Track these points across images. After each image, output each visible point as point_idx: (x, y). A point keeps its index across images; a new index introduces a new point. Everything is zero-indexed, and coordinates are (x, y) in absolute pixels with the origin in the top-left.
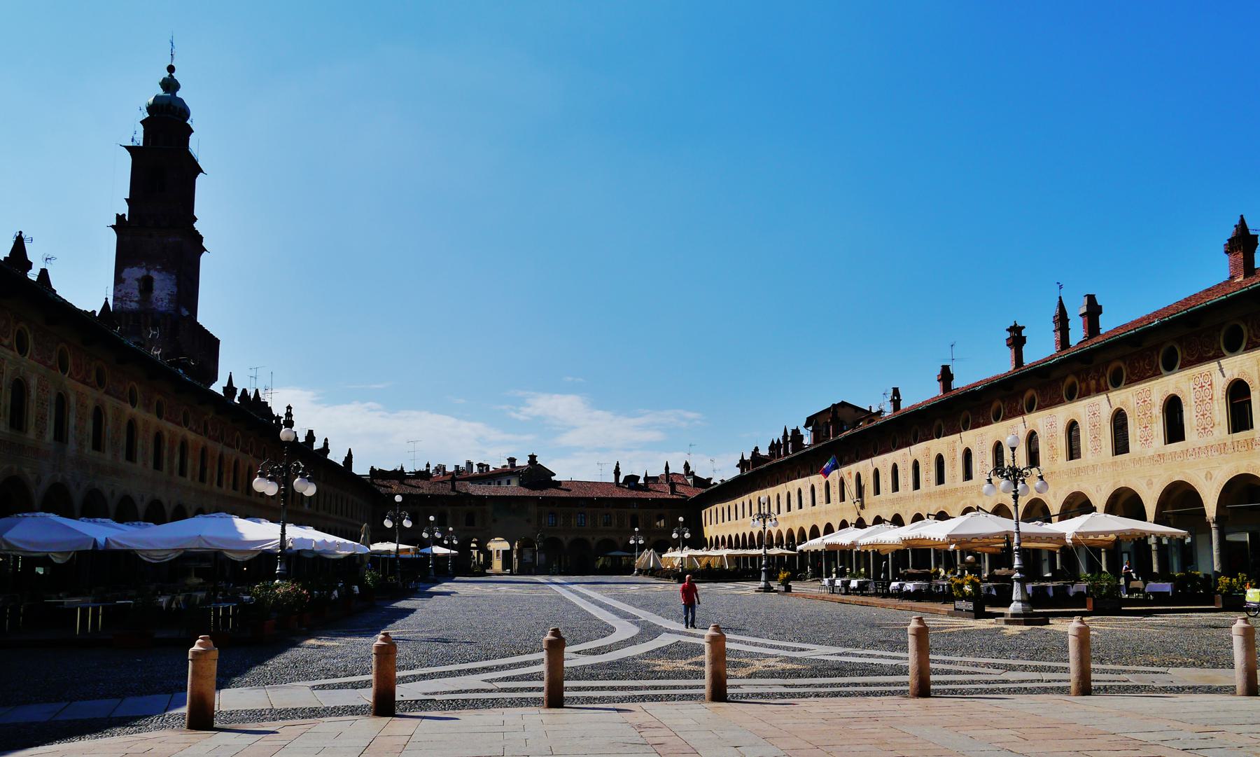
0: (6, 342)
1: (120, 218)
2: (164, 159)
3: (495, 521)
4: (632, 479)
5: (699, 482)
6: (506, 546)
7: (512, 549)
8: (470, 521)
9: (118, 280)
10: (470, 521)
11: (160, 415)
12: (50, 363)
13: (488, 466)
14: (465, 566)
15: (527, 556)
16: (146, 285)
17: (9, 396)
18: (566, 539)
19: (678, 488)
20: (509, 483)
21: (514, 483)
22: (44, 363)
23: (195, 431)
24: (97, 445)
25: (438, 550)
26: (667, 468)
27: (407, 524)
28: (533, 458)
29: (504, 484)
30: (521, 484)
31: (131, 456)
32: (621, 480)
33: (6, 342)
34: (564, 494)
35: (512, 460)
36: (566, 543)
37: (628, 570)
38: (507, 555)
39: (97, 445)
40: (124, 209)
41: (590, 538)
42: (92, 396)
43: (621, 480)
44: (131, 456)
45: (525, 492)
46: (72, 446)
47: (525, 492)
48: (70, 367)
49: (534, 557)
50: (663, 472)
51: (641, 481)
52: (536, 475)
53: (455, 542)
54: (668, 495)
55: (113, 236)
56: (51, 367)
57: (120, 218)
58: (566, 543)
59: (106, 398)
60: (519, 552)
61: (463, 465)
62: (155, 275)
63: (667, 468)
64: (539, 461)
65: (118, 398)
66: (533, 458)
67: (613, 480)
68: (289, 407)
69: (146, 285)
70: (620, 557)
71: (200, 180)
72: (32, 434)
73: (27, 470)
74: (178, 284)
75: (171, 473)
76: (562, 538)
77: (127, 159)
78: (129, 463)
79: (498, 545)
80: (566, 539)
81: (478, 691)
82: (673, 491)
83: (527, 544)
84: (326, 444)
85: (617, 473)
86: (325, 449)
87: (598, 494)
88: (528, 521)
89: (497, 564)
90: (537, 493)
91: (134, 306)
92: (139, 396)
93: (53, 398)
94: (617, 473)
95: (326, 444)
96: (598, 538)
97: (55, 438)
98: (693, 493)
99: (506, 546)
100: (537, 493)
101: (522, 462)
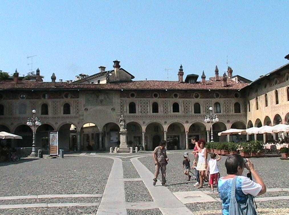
3: (86, 109)
4: (192, 78)
5: (240, 79)
8: (67, 109)
10: (67, 109)
21: (104, 82)
26: (217, 72)
28: (117, 64)
32: (184, 81)
50: (214, 75)
51: (199, 79)
63: (217, 72)
66: (117, 64)
76: (140, 122)
85: (181, 73)
87: (166, 88)
88: (113, 109)
94: (181, 73)
98: (241, 86)
101: (110, 67)
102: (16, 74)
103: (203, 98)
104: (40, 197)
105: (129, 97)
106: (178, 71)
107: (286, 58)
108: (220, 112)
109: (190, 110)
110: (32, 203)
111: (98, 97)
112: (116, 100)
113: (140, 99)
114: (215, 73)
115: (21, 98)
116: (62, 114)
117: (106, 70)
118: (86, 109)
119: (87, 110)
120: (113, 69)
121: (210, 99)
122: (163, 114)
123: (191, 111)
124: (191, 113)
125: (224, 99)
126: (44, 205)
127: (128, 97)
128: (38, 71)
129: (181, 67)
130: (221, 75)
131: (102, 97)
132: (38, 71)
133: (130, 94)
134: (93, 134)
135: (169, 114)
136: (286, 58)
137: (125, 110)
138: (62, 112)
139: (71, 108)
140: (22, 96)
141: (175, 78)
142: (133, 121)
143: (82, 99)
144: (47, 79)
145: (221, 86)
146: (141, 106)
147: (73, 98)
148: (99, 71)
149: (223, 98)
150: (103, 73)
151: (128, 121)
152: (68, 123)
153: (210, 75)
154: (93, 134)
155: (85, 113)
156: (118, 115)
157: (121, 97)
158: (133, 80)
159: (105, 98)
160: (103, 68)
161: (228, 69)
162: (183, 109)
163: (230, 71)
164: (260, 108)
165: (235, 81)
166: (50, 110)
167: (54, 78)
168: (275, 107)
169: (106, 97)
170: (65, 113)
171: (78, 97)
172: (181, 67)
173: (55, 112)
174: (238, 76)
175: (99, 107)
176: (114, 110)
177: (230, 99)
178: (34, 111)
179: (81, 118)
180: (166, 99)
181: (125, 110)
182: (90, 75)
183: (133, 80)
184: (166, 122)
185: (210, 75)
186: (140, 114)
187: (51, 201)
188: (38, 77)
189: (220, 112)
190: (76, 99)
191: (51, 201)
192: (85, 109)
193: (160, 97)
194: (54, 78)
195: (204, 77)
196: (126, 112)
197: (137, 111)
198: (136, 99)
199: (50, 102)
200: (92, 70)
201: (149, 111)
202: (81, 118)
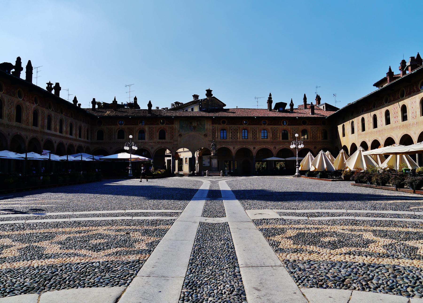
3: (180, 135)
4: (281, 106)
5: (329, 107)
6: (189, 155)
7: (193, 156)
8: (162, 136)
10: (162, 136)
15: (206, 162)
18: (234, 149)
19: (316, 111)
20: (192, 109)
21: (196, 109)
25: (122, 156)
26: (305, 99)
28: (209, 93)
30: (201, 109)
32: (273, 108)
34: (231, 115)
35: (196, 96)
36: (234, 151)
37: (292, 173)
38: (192, 161)
41: (251, 148)
43: (273, 108)
45: (204, 114)
47: (204, 114)
49: (210, 162)
51: (288, 107)
52: (211, 104)
53: (135, 148)
54: (310, 115)
58: (234, 151)
60: (200, 158)
63: (305, 99)
64: (215, 94)
66: (209, 93)
67: (266, 107)
70: (275, 161)
76: (231, 148)
79: (185, 154)
80: (234, 149)
82: (313, 113)
83: (205, 153)
85: (270, 101)
87: (255, 115)
88: (205, 135)
89: (186, 168)
90: (211, 115)
94: (270, 101)
96: (258, 147)
99: (189, 155)
100: (211, 115)
101: (203, 96)
102: (115, 102)
103: (291, 125)
104: (127, 211)
105: (221, 124)
106: (267, 99)
107: (374, 85)
108: (267, 138)
109: (278, 137)
110: (120, 215)
111: (191, 123)
112: (208, 126)
113: (230, 126)
114: (303, 101)
115: (119, 124)
116: (157, 139)
117: (200, 98)
118: (180, 135)
119: (181, 135)
120: (206, 97)
121: (298, 126)
122: (251, 140)
123: (279, 138)
124: (278, 140)
125: (311, 126)
126: (130, 218)
127: (220, 124)
129: (270, 95)
130: (308, 102)
131: (194, 124)
132: (135, 99)
133: (221, 121)
134: (186, 158)
135: (258, 140)
136: (374, 85)
137: (216, 136)
138: (158, 137)
139: (167, 134)
140: (120, 123)
141: (266, 107)
142: (224, 146)
143: (176, 126)
144: (143, 106)
145: (308, 113)
146: (231, 133)
147: (168, 124)
148: (192, 99)
149: (310, 125)
150: (196, 100)
151: (218, 147)
152: (163, 147)
153: (298, 103)
154: (186, 158)
155: (179, 139)
156: (209, 141)
157: (213, 124)
158: (224, 108)
159: (198, 124)
160: (196, 96)
161: (317, 98)
162: (271, 136)
163: (318, 99)
164: (347, 135)
165: (322, 108)
167: (150, 105)
168: (361, 134)
169: (199, 123)
171: (173, 124)
172: (270, 95)
173: (151, 138)
174: (326, 104)
175: (192, 133)
176: (206, 136)
177: (318, 126)
178: (131, 137)
179: (176, 143)
180: (255, 126)
181: (216, 136)
182: (184, 103)
183: (224, 108)
184: (254, 148)
185: (298, 103)
186: (231, 140)
187: (136, 214)
188: (134, 105)
189: (267, 138)
190: (171, 126)
191: (136, 214)
192: (179, 135)
193: (249, 124)
194: (150, 105)
195: (292, 105)
196: (218, 137)
197: (228, 137)
198: (227, 126)
199: (147, 128)
201: (239, 137)
202: (176, 143)
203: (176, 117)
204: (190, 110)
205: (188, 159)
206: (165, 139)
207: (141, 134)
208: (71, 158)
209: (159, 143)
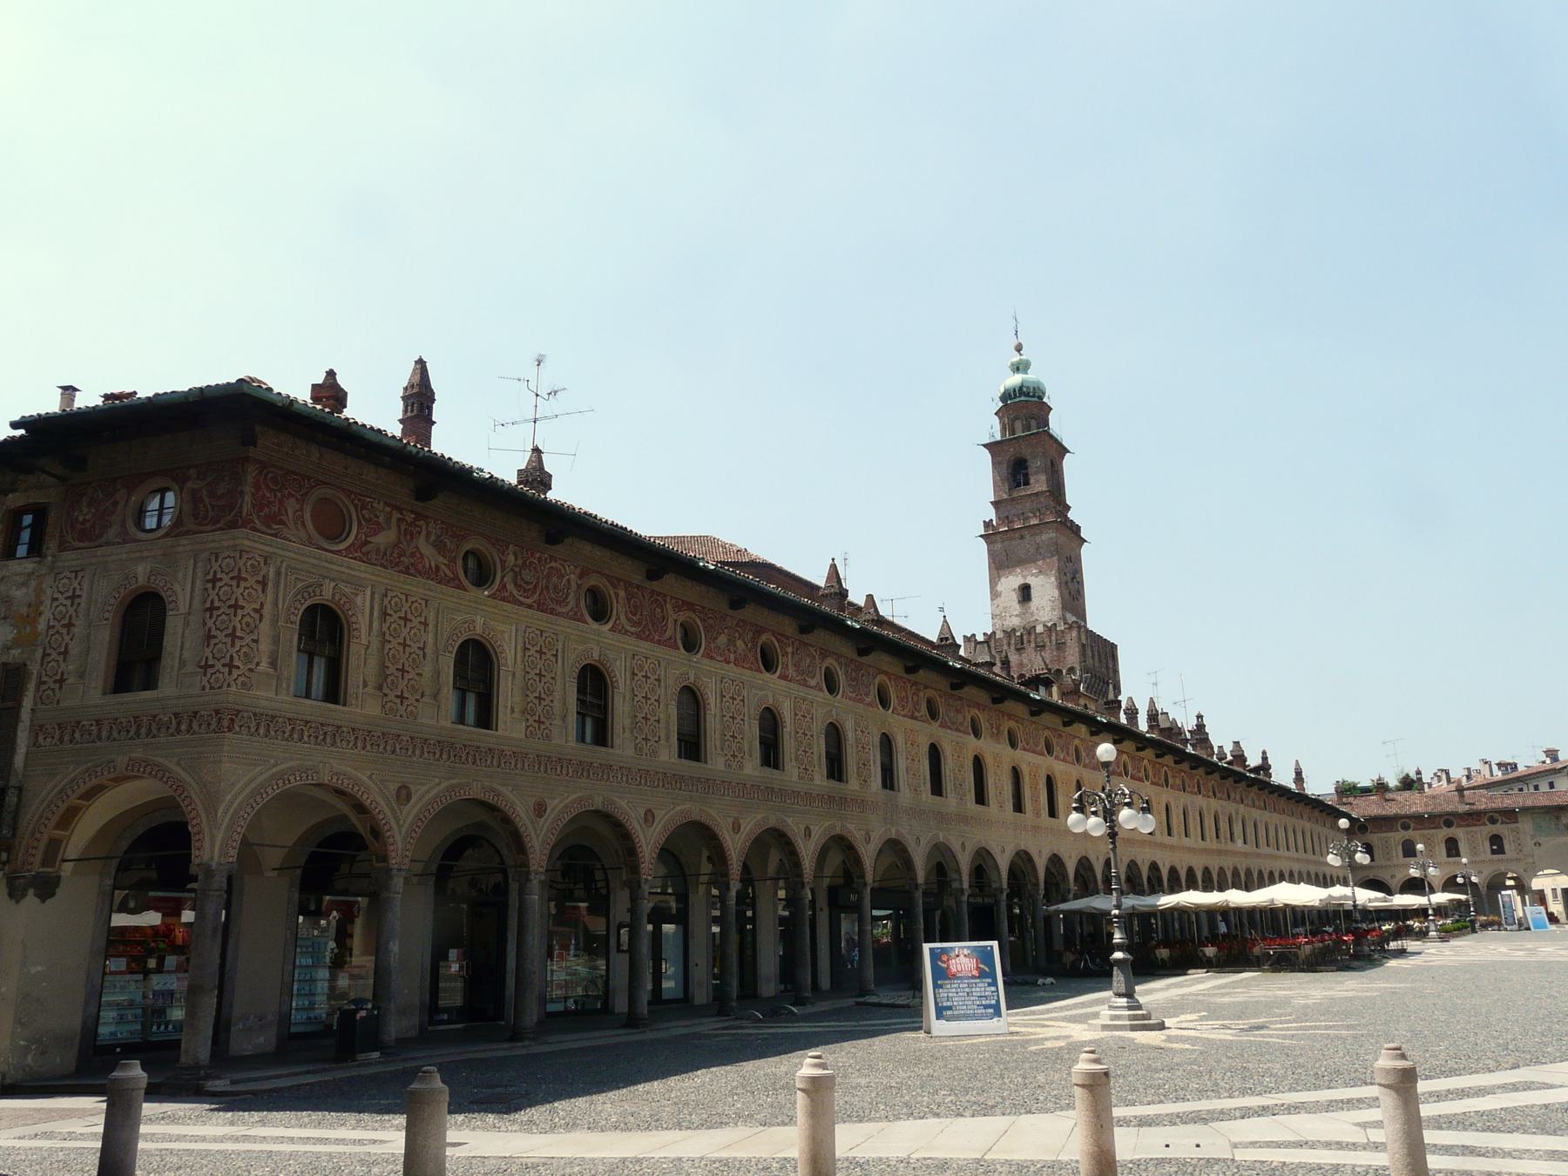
0: (813, 683)
1: (987, 524)
2: (1027, 450)
3: (1538, 844)
8: (1497, 843)
9: (995, 594)
10: (1497, 843)
11: (1013, 745)
12: (868, 700)
13: (1514, 767)
14: (1477, 911)
16: (1025, 593)
17: (823, 742)
20: (1552, 785)
22: (861, 701)
23: (1064, 760)
24: (937, 789)
27: (1362, 858)
29: (1544, 787)
31: (981, 798)
33: (813, 683)
39: (937, 789)
40: (991, 514)
42: (926, 732)
44: (981, 798)
46: (904, 795)
48: (894, 700)
55: (983, 544)
56: (869, 705)
57: (987, 524)
59: (942, 732)
61: (1476, 765)
62: (1031, 580)
65: (957, 730)
68: (1200, 717)
69: (1025, 593)
71: (1067, 462)
72: (853, 784)
73: (852, 827)
74: (1060, 587)
75: (1038, 814)
77: (986, 456)
78: (980, 808)
81: (1340, 1146)
84: (1265, 758)
86: (1265, 767)
91: (1015, 622)
92: (984, 726)
93: (877, 739)
95: (1265, 758)
97: (885, 786)
111: (1558, 818)
128: (1419, 773)
132: (1419, 773)
134: (1554, 890)
143: (1526, 825)
154: (1554, 890)
166: (1462, 847)
170: (1493, 852)
199: (1459, 833)
200: (1529, 759)
203: (1525, 810)
204: (1544, 787)
205: (1559, 892)
206: (1501, 851)
207: (1452, 848)
208: (1236, 897)
209: (1492, 861)
